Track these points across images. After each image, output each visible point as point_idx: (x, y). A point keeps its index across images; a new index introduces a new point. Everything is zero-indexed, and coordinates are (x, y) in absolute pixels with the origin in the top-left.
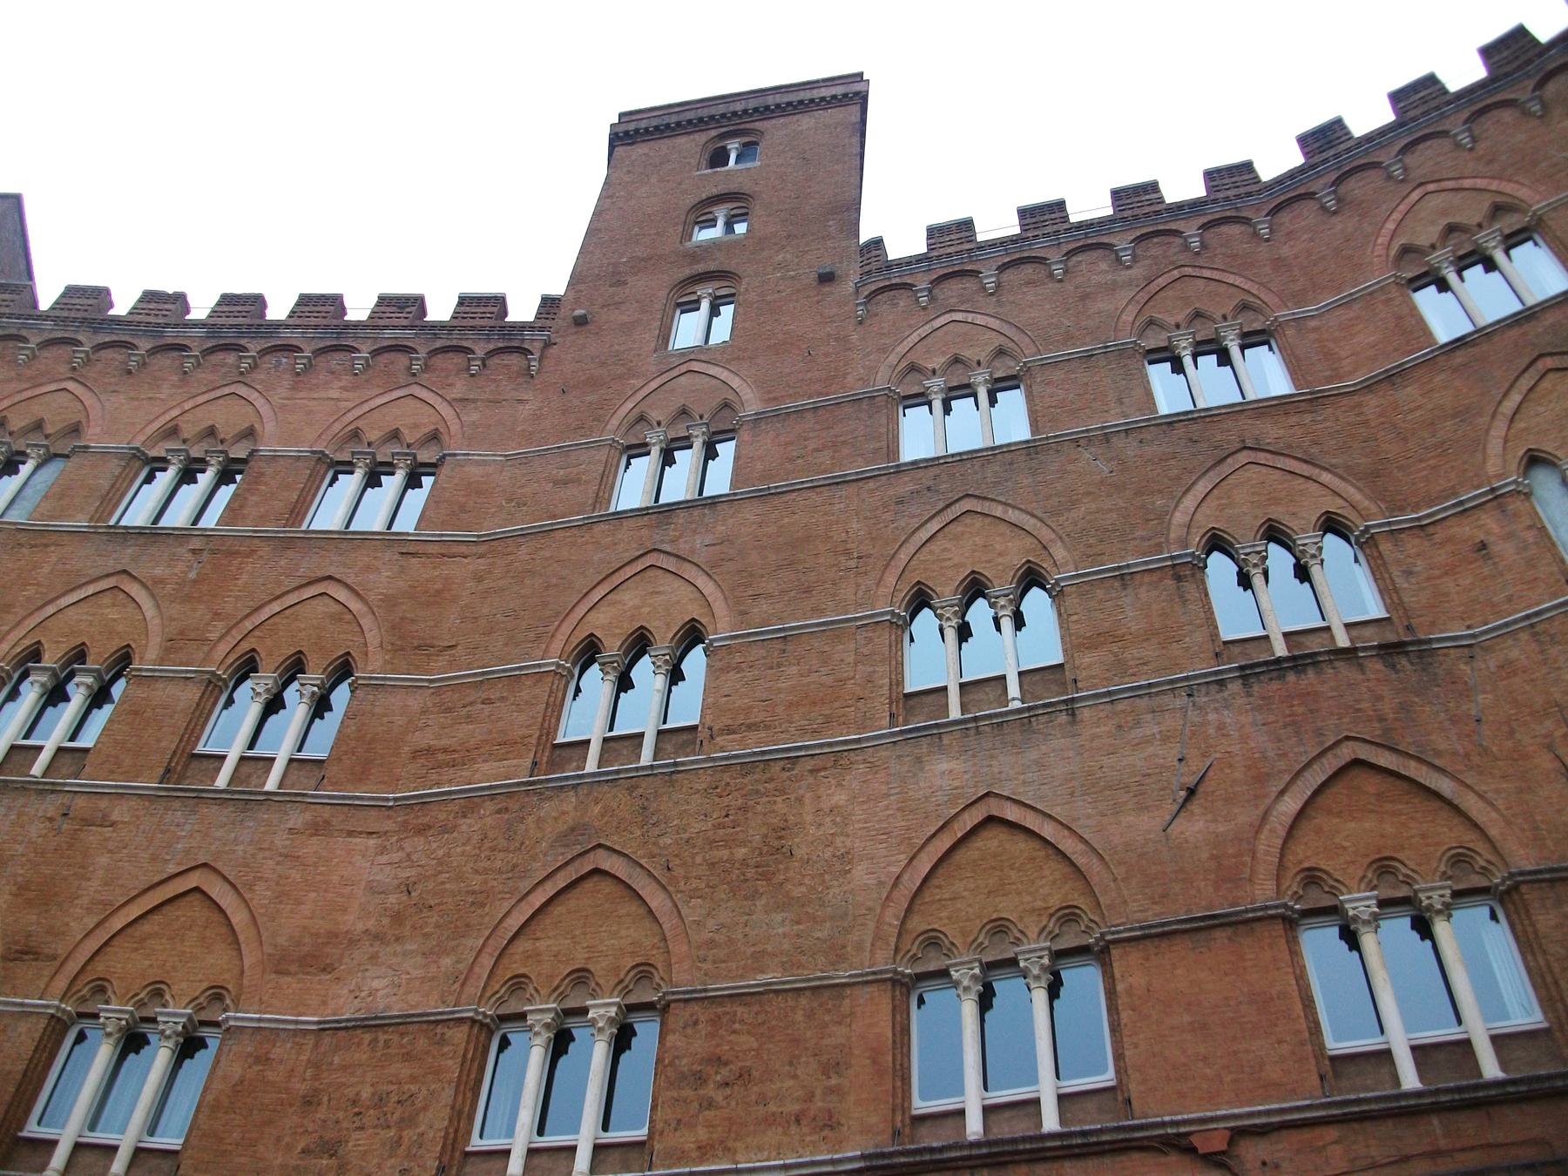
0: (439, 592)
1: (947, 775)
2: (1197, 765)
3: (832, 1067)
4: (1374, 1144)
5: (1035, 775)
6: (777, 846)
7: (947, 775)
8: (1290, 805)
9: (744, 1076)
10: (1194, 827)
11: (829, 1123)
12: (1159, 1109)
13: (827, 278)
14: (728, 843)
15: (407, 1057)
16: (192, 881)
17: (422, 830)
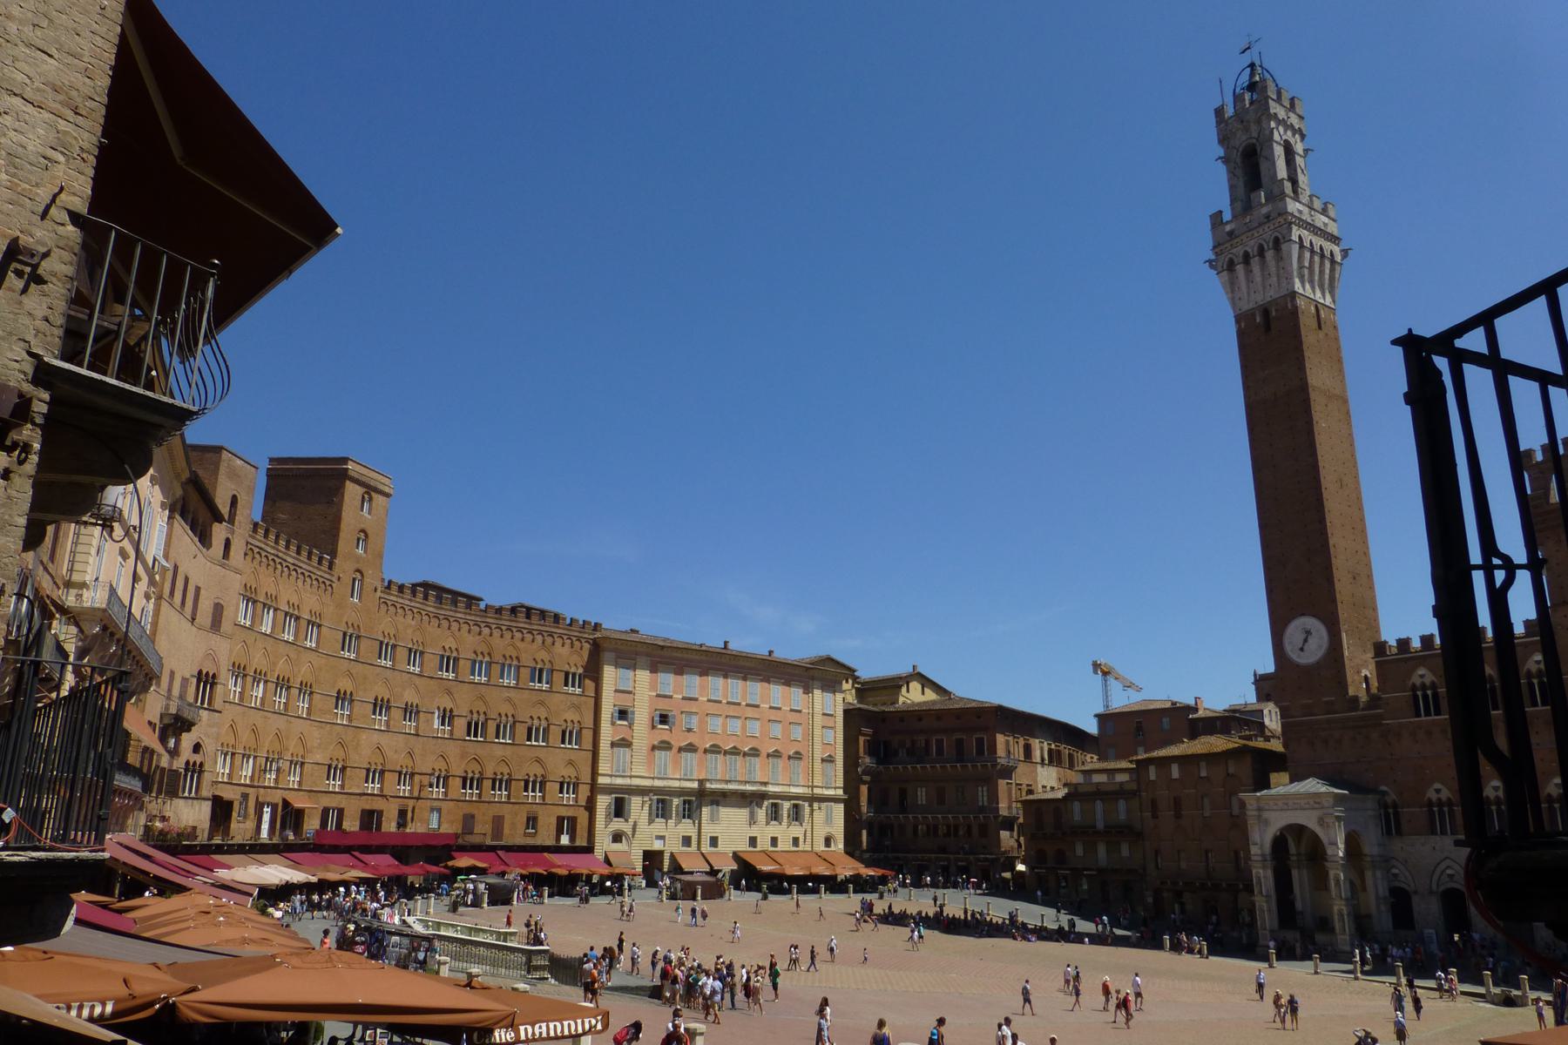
1: (376, 737)
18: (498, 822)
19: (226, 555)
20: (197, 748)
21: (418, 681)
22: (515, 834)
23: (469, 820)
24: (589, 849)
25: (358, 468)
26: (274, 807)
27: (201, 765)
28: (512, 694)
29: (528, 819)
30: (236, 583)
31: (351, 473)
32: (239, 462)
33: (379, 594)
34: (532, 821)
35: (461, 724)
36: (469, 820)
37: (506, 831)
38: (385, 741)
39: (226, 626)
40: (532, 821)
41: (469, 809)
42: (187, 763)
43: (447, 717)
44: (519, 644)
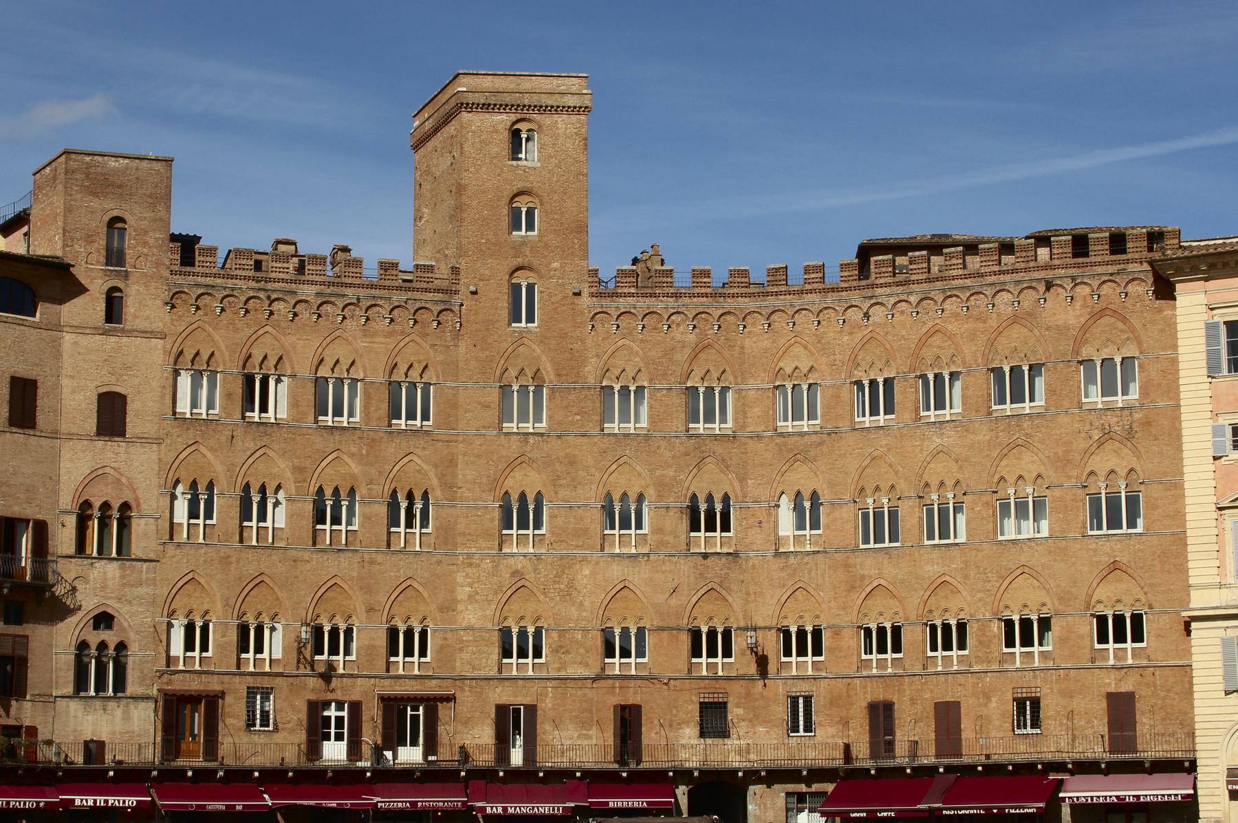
0: (451, 461)
1: (616, 571)
2: (676, 582)
3: (587, 651)
4: (695, 684)
5: (637, 576)
6: (571, 585)
7: (616, 571)
8: (695, 599)
9: (568, 652)
10: (673, 601)
11: (587, 665)
12: (655, 672)
13: (578, 294)
14: (558, 583)
15: (483, 639)
16: (409, 582)
17: (470, 565)
18: (947, 717)
19: (113, 308)
20: (104, 620)
21: (719, 449)
22: (991, 738)
23: (882, 716)
24: (1188, 767)
25: (487, 83)
26: (356, 708)
27: (122, 646)
28: (949, 438)
29: (1020, 703)
30: (156, 354)
31: (471, 98)
32: (113, 163)
33: (585, 300)
34: (1028, 710)
35: (840, 522)
36: (882, 716)
37: (967, 733)
38: (637, 576)
39: (133, 424)
40: (1028, 710)
41: (879, 693)
42: (83, 646)
43: (809, 510)
44: (952, 327)
